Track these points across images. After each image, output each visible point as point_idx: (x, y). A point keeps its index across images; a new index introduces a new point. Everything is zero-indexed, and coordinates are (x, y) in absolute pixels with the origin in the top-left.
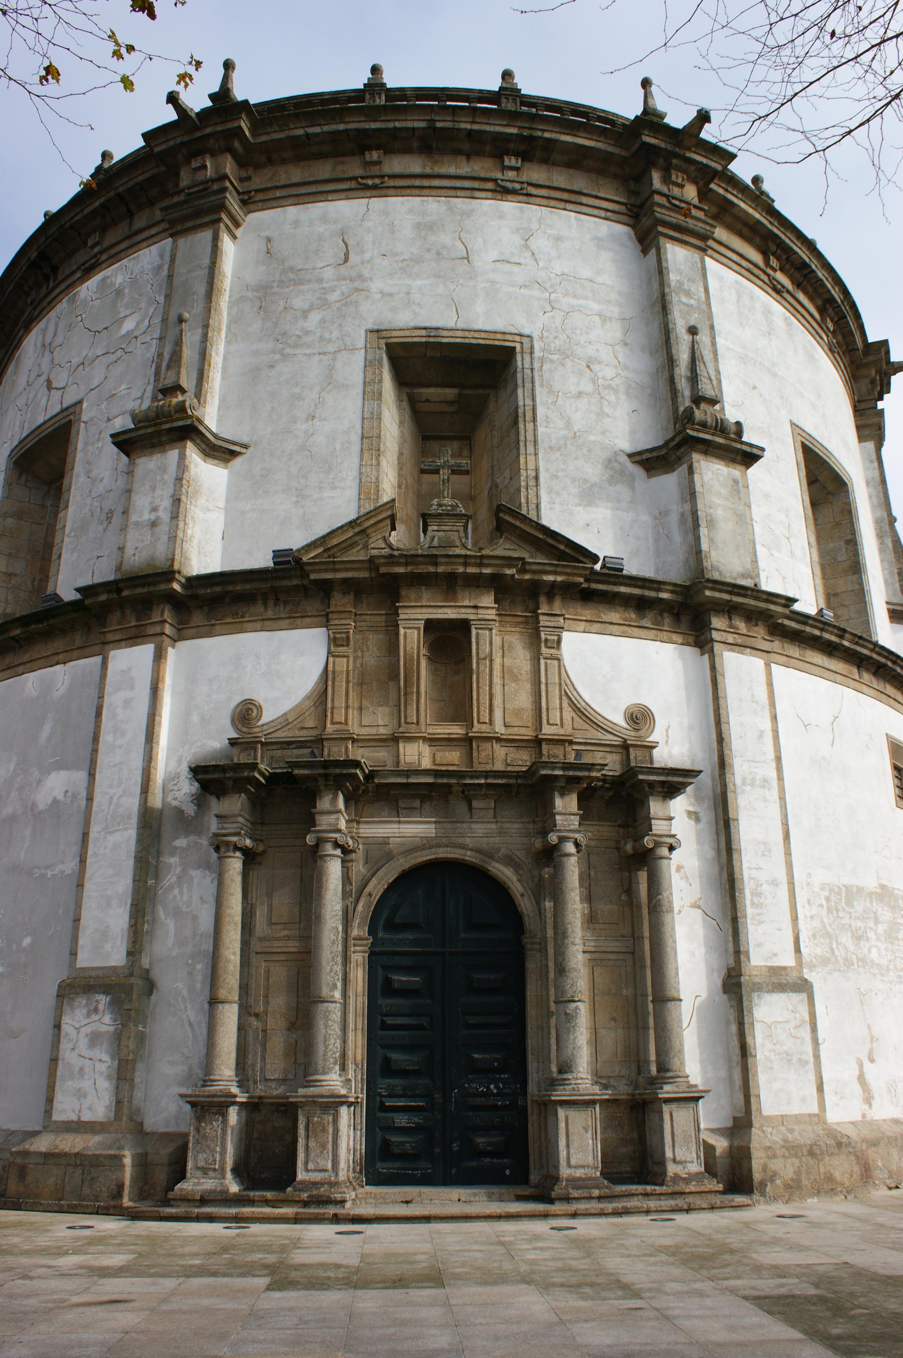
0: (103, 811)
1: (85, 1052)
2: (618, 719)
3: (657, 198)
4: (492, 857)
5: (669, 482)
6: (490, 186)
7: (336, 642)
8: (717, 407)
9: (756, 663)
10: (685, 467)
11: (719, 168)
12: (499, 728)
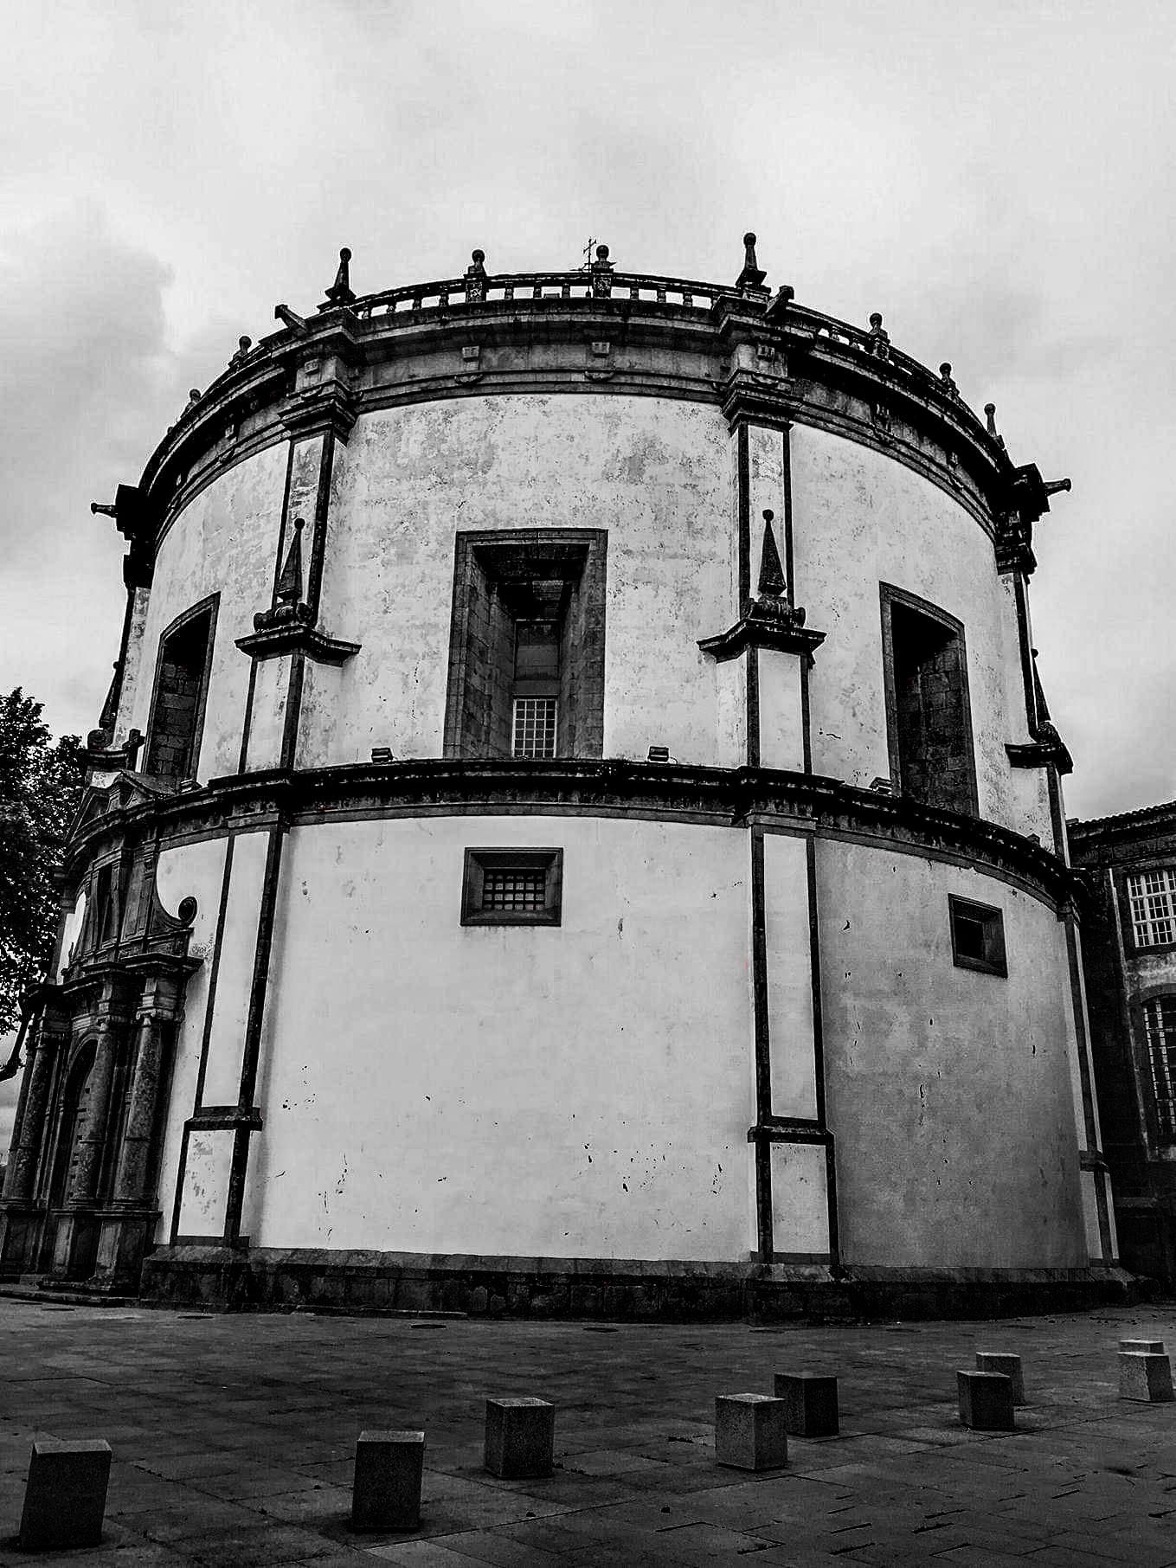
8: (784, 594)
10: (744, 656)
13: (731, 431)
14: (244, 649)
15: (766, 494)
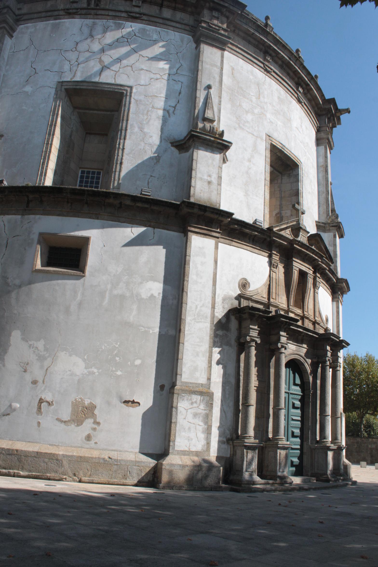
0: (193, 311)
1: (191, 420)
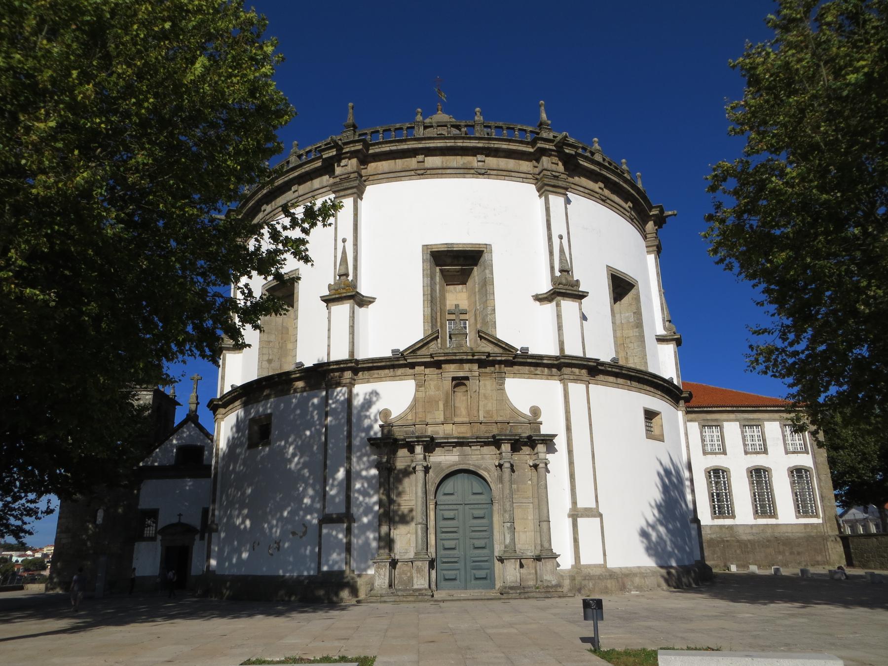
2: (527, 412)
3: (545, 172)
4: (479, 467)
5: (550, 307)
6: (472, 171)
7: (418, 386)
9: (581, 387)
10: (554, 303)
11: (573, 153)
12: (481, 419)
13: (540, 196)
14: (325, 301)
15: (558, 228)
